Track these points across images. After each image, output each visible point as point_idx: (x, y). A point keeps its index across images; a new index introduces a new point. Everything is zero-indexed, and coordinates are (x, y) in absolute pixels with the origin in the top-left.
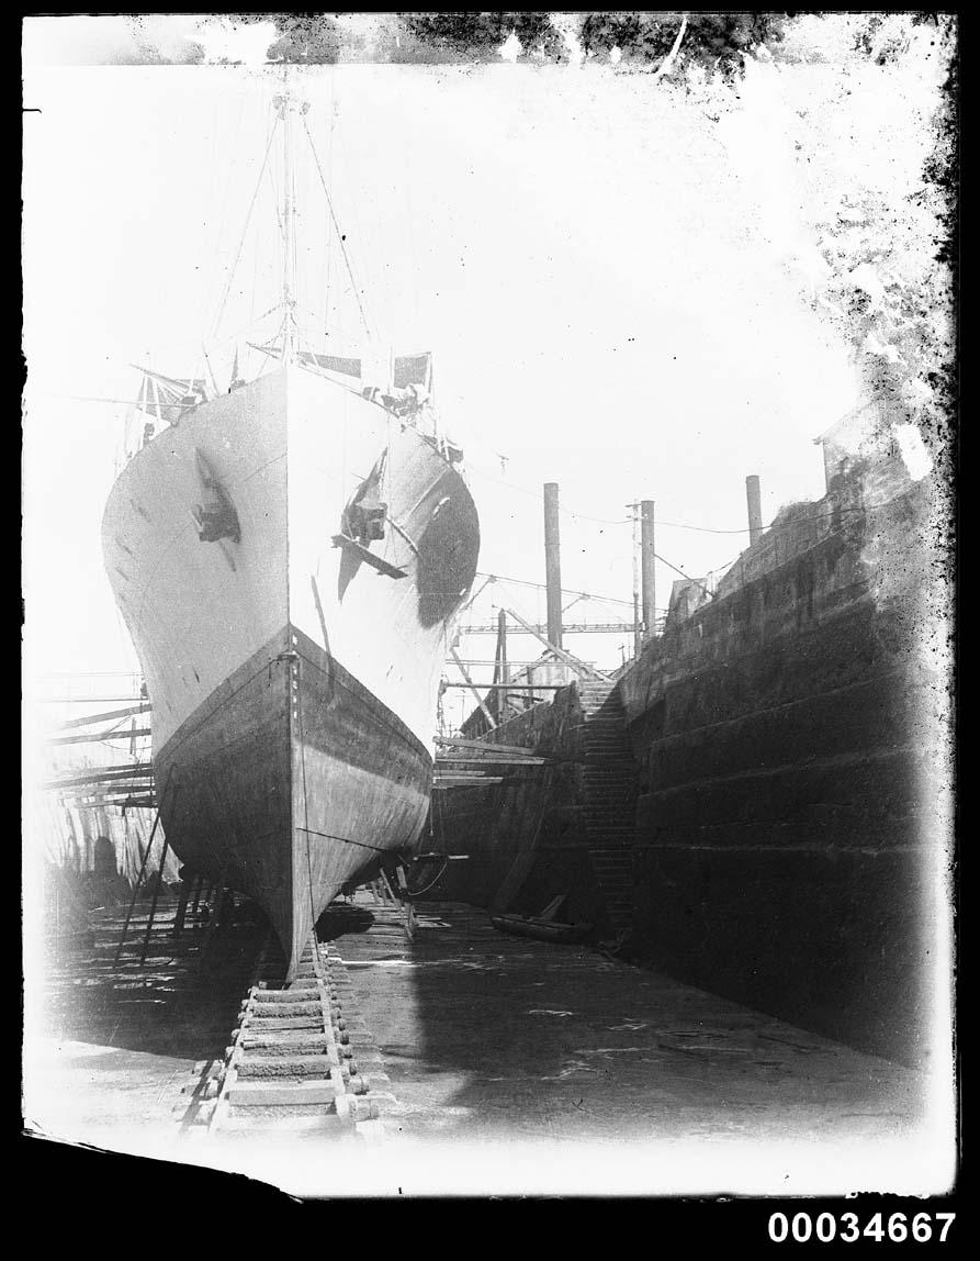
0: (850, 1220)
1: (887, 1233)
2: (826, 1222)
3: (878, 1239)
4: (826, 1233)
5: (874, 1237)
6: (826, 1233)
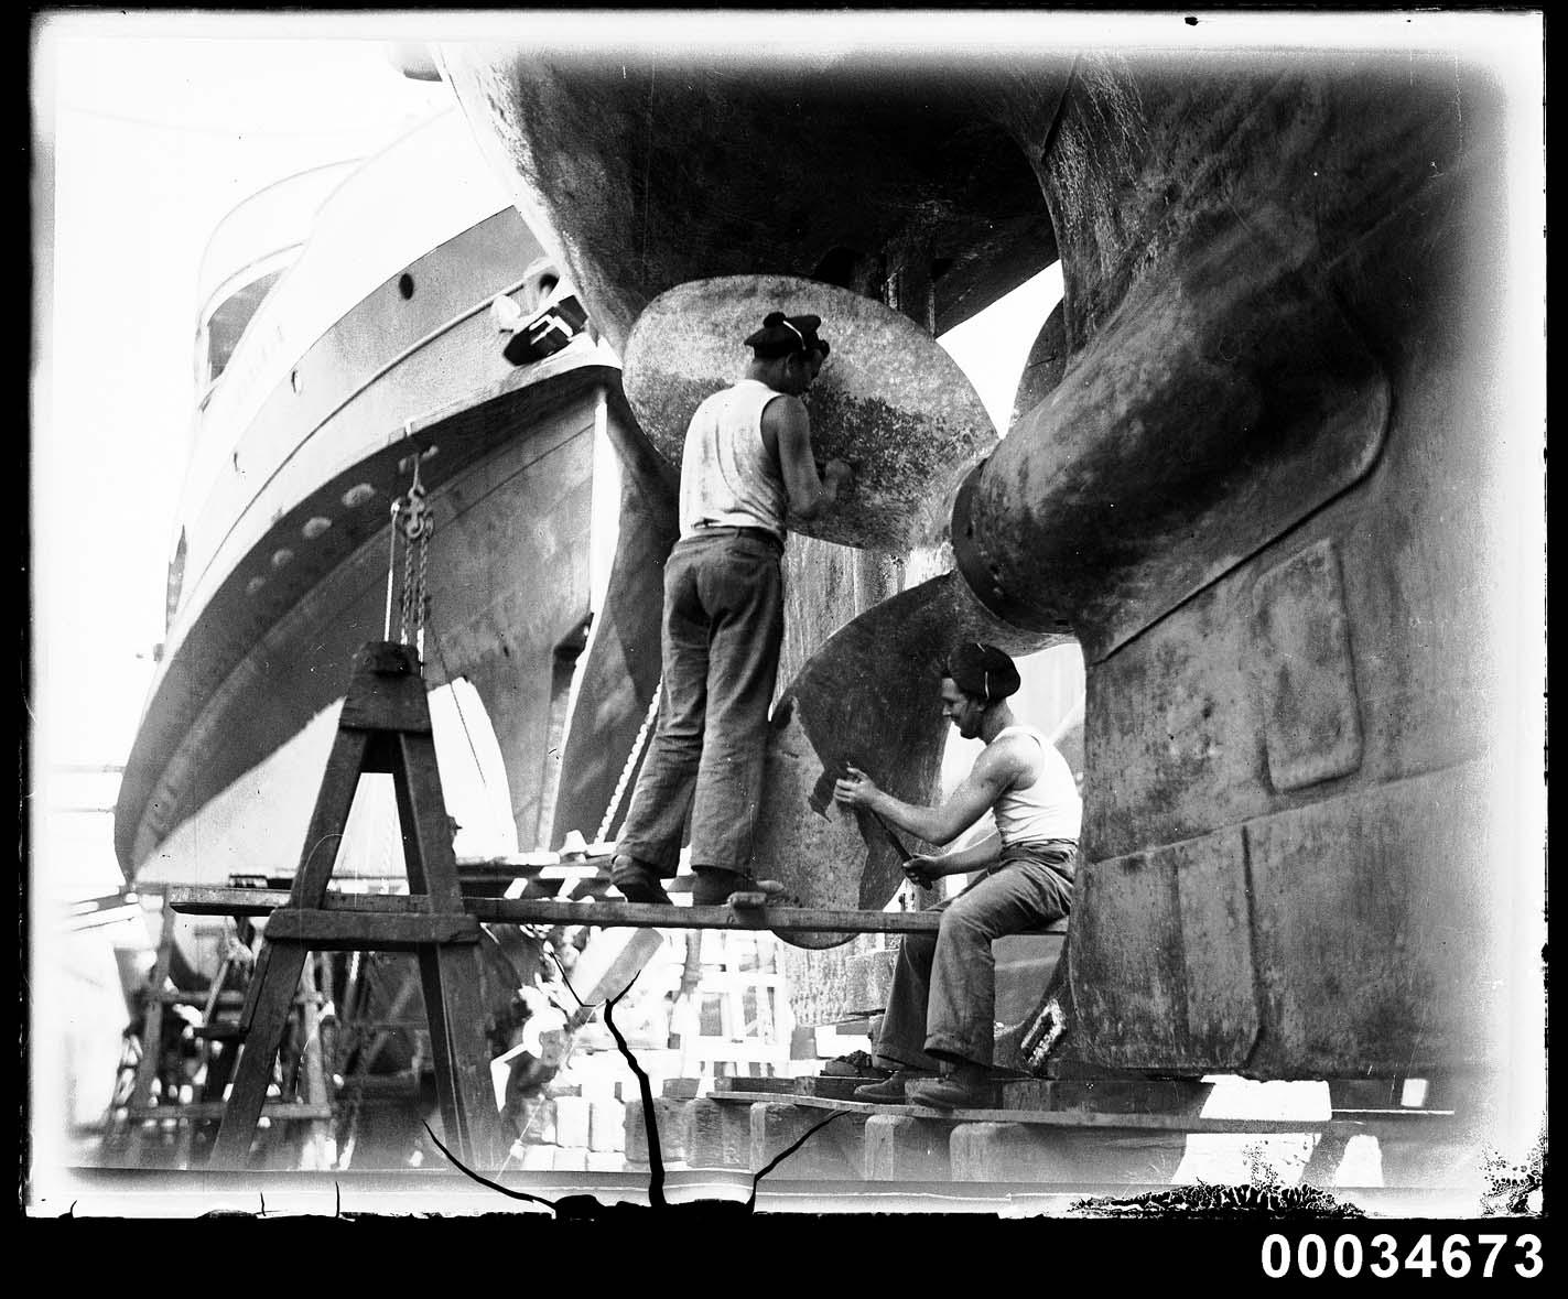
0: (1384, 1246)
1: (1440, 1264)
2: (1348, 1248)
3: (1427, 1274)
4: (1348, 1264)
5: (1420, 1271)
6: (1348, 1264)
